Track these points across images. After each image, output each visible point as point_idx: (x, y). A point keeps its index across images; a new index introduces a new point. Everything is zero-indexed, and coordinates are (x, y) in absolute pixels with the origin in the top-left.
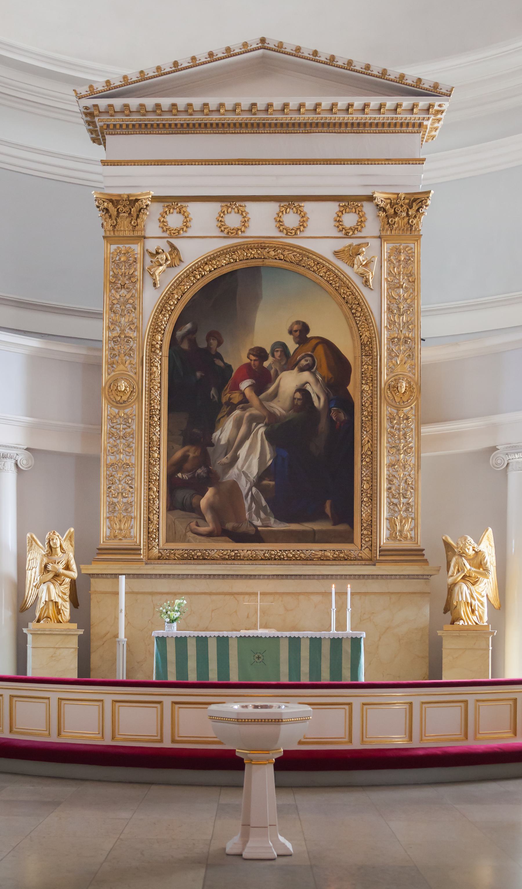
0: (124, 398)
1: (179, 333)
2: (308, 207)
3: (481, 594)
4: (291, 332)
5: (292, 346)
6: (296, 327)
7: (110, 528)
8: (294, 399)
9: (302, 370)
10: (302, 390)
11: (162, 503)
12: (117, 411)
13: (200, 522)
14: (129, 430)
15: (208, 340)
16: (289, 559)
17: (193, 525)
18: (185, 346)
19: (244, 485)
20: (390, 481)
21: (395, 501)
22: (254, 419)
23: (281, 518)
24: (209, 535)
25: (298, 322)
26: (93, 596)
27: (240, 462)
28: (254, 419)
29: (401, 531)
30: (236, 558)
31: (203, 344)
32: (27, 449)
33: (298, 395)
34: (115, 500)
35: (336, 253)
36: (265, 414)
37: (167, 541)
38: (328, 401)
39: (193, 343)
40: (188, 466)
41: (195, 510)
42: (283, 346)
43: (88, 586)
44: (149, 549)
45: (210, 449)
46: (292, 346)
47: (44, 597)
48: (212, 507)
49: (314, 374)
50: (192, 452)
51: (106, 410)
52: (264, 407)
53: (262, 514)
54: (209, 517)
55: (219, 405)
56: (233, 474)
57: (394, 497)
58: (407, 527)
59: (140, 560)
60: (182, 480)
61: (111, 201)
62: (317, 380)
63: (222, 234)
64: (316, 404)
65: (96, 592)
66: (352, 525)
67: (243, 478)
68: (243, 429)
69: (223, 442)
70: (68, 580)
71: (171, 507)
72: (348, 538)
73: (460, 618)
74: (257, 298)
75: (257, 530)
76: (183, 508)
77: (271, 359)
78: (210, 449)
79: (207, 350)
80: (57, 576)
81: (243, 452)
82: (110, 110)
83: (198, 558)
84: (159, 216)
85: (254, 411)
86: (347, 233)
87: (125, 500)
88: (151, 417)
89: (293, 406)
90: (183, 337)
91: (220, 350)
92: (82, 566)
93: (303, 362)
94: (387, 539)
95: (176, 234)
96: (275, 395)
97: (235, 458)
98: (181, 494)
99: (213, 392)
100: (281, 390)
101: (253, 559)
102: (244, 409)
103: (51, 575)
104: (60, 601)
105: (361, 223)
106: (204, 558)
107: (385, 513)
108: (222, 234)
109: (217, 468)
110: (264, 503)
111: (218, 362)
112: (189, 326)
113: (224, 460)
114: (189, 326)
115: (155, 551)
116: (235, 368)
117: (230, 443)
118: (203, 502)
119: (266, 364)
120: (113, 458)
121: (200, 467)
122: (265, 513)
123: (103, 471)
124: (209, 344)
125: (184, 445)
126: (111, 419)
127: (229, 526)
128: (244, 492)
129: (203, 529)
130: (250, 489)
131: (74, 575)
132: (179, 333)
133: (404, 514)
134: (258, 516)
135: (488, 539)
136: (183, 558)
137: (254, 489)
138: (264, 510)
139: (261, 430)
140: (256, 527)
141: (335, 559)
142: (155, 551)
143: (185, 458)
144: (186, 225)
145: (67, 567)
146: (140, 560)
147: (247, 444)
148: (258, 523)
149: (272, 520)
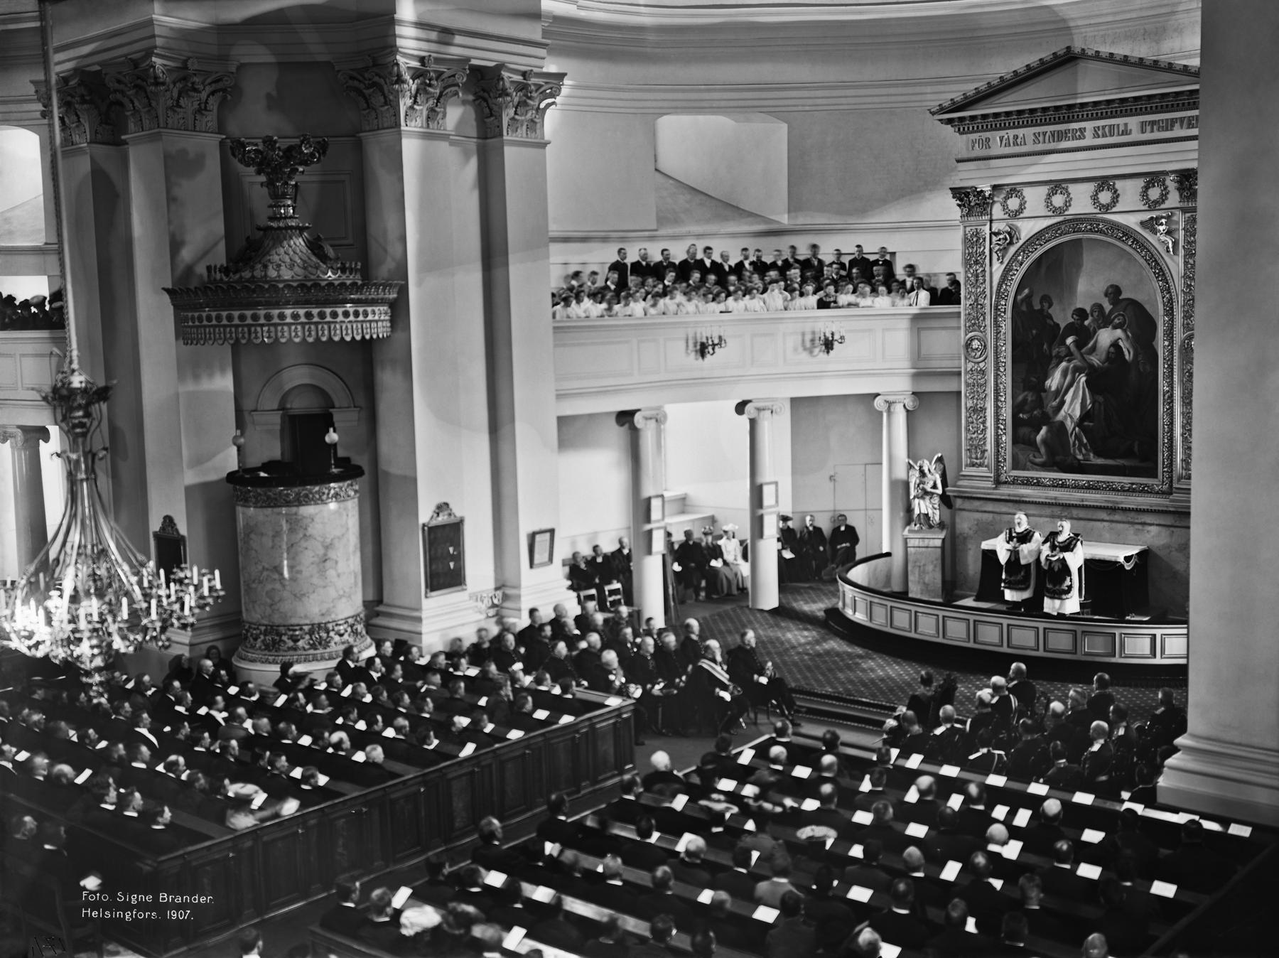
1: (1019, 298)
2: (1119, 184)
4: (1106, 295)
5: (1108, 307)
6: (1110, 290)
8: (1108, 352)
9: (1115, 328)
10: (1115, 344)
11: (1007, 439)
13: (1036, 454)
15: (1041, 303)
17: (1031, 457)
18: (1024, 308)
19: (1069, 425)
22: (1077, 370)
23: (1098, 454)
25: (1112, 286)
27: (1066, 407)
28: (1077, 370)
31: (1037, 307)
33: (1112, 350)
35: (1142, 223)
36: (1086, 365)
38: (1136, 355)
39: (1030, 305)
40: (1027, 408)
41: (1032, 444)
42: (1099, 307)
45: (1043, 395)
46: (1108, 307)
48: (1044, 441)
49: (1125, 331)
50: (1030, 397)
52: (1084, 358)
54: (1043, 450)
55: (1050, 358)
60: (1023, 419)
62: (1128, 336)
63: (1051, 213)
64: (1127, 357)
68: (1069, 378)
69: (1053, 388)
71: (1015, 441)
74: (1079, 266)
75: (1080, 464)
76: (1024, 443)
77: (1090, 318)
78: (1043, 395)
79: (1042, 310)
81: (1068, 398)
83: (1034, 484)
85: (1076, 362)
86: (1153, 205)
89: (1108, 358)
90: (1022, 300)
91: (1050, 311)
93: (1116, 321)
95: (1016, 214)
96: (1094, 349)
97: (1062, 403)
98: (1024, 431)
99: (1045, 347)
100: (1099, 345)
101: (1077, 487)
102: (1069, 361)
105: (1164, 197)
108: (1051, 213)
109: (1049, 410)
110: (1085, 441)
111: (1049, 321)
112: (1026, 291)
113: (1054, 404)
114: (1026, 291)
116: (1062, 326)
117: (1058, 391)
118: (1039, 438)
119: (1086, 323)
121: (1035, 409)
122: (1086, 449)
124: (1042, 306)
125: (1024, 391)
127: (1058, 458)
129: (1038, 460)
130: (1074, 429)
132: (1019, 298)
134: (1081, 451)
138: (1085, 446)
139: (1083, 379)
140: (1079, 460)
143: (1025, 400)
144: (1022, 208)
147: (1072, 390)
148: (1080, 457)
149: (1092, 455)
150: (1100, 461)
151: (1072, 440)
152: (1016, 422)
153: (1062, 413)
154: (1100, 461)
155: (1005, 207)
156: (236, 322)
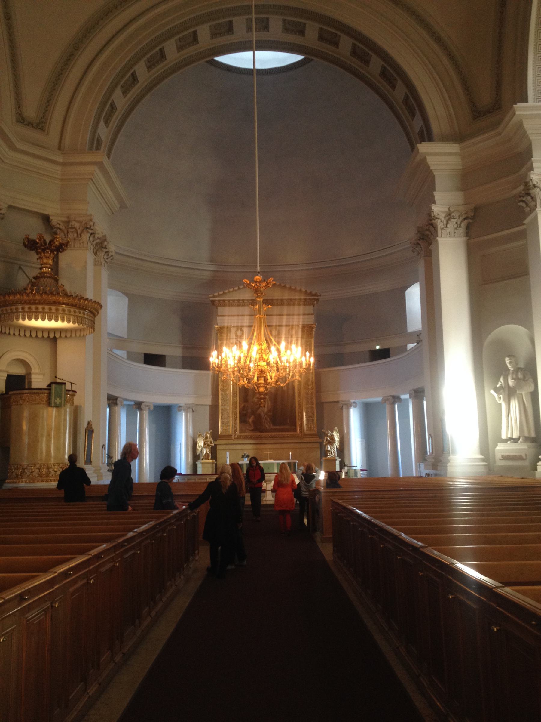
0: (226, 388)
3: (334, 448)
7: (222, 429)
12: (223, 392)
14: (227, 398)
16: (277, 437)
17: (247, 428)
19: (263, 415)
20: (306, 412)
21: (309, 419)
23: (274, 424)
24: (252, 430)
26: (218, 452)
29: (311, 428)
30: (261, 437)
32: (196, 405)
34: (224, 420)
37: (240, 432)
43: (216, 447)
44: (234, 436)
47: (205, 452)
48: (253, 421)
51: (220, 392)
53: (268, 423)
54: (252, 425)
56: (259, 411)
57: (308, 417)
58: (312, 427)
59: (232, 439)
61: (220, 328)
65: (219, 450)
66: (295, 426)
67: (262, 412)
70: (211, 447)
71: (241, 422)
72: (295, 430)
73: (328, 455)
80: (208, 445)
82: (219, 301)
83: (249, 438)
84: (234, 331)
87: (226, 420)
88: (234, 394)
92: (214, 442)
94: (307, 431)
101: (266, 438)
103: (206, 445)
104: (208, 453)
106: (251, 438)
107: (305, 422)
110: (269, 420)
115: (236, 436)
120: (222, 407)
123: (220, 412)
126: (222, 395)
128: (263, 417)
129: (251, 429)
130: (265, 416)
131: (213, 445)
133: (311, 423)
134: (267, 424)
135: (336, 431)
136: (245, 438)
137: (266, 416)
140: (267, 428)
141: (291, 437)
142: (236, 436)
145: (211, 443)
146: (232, 439)
148: (267, 426)
149: (272, 425)
150: (275, 427)
151: (264, 420)
152: (241, 415)
153: (260, 410)
154: (275, 427)
155: (236, 335)
156: (5, 312)
